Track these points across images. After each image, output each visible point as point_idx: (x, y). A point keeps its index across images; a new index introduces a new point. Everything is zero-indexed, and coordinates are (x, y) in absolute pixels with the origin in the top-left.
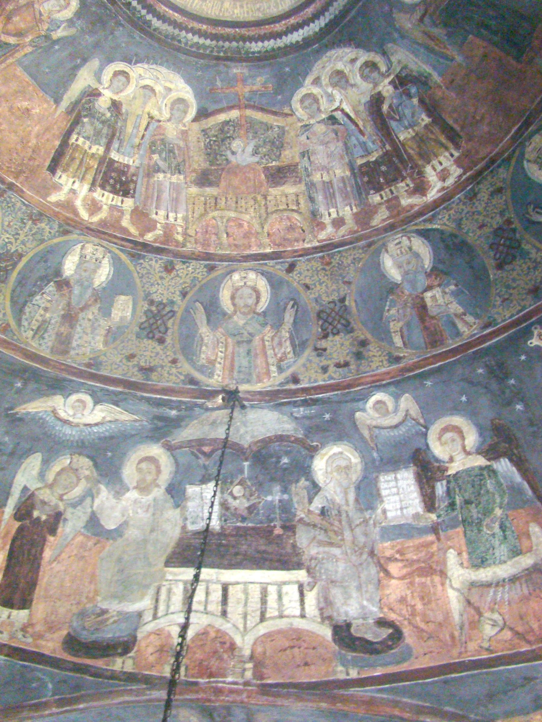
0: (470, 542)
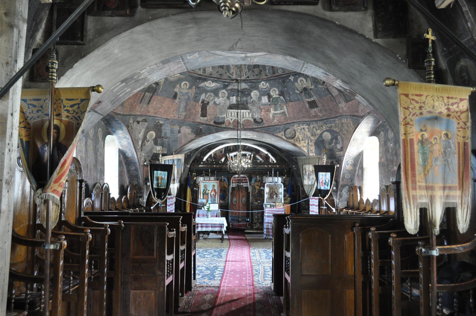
0: (275, 107)
